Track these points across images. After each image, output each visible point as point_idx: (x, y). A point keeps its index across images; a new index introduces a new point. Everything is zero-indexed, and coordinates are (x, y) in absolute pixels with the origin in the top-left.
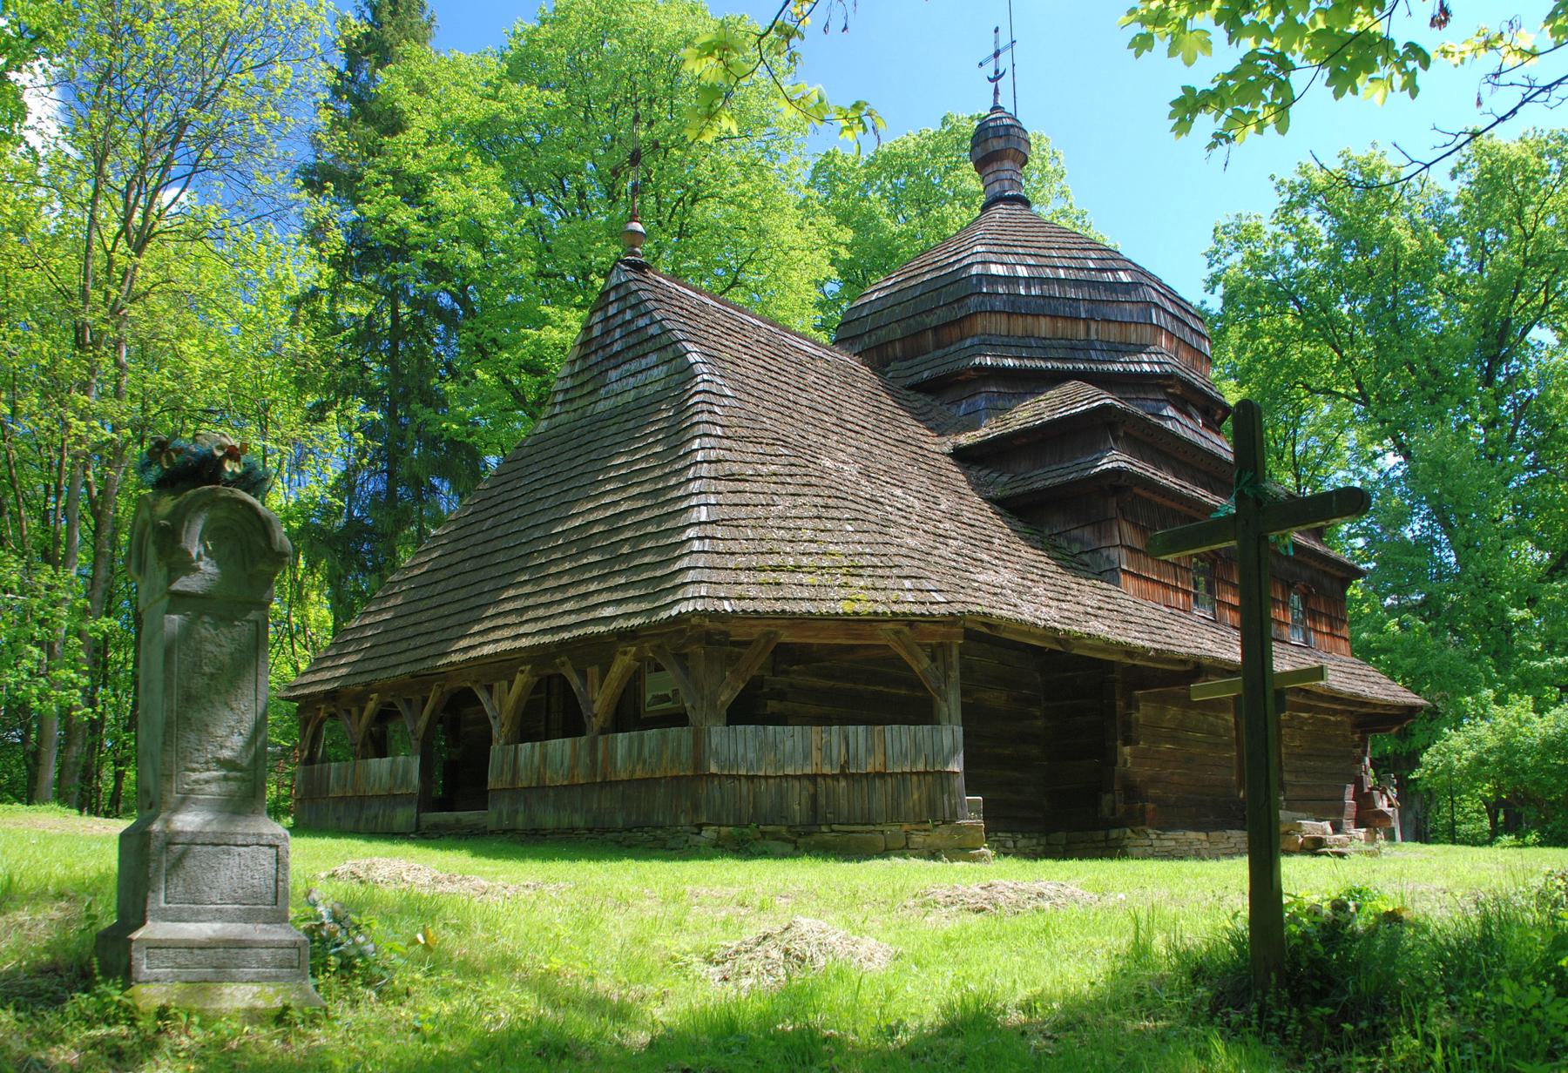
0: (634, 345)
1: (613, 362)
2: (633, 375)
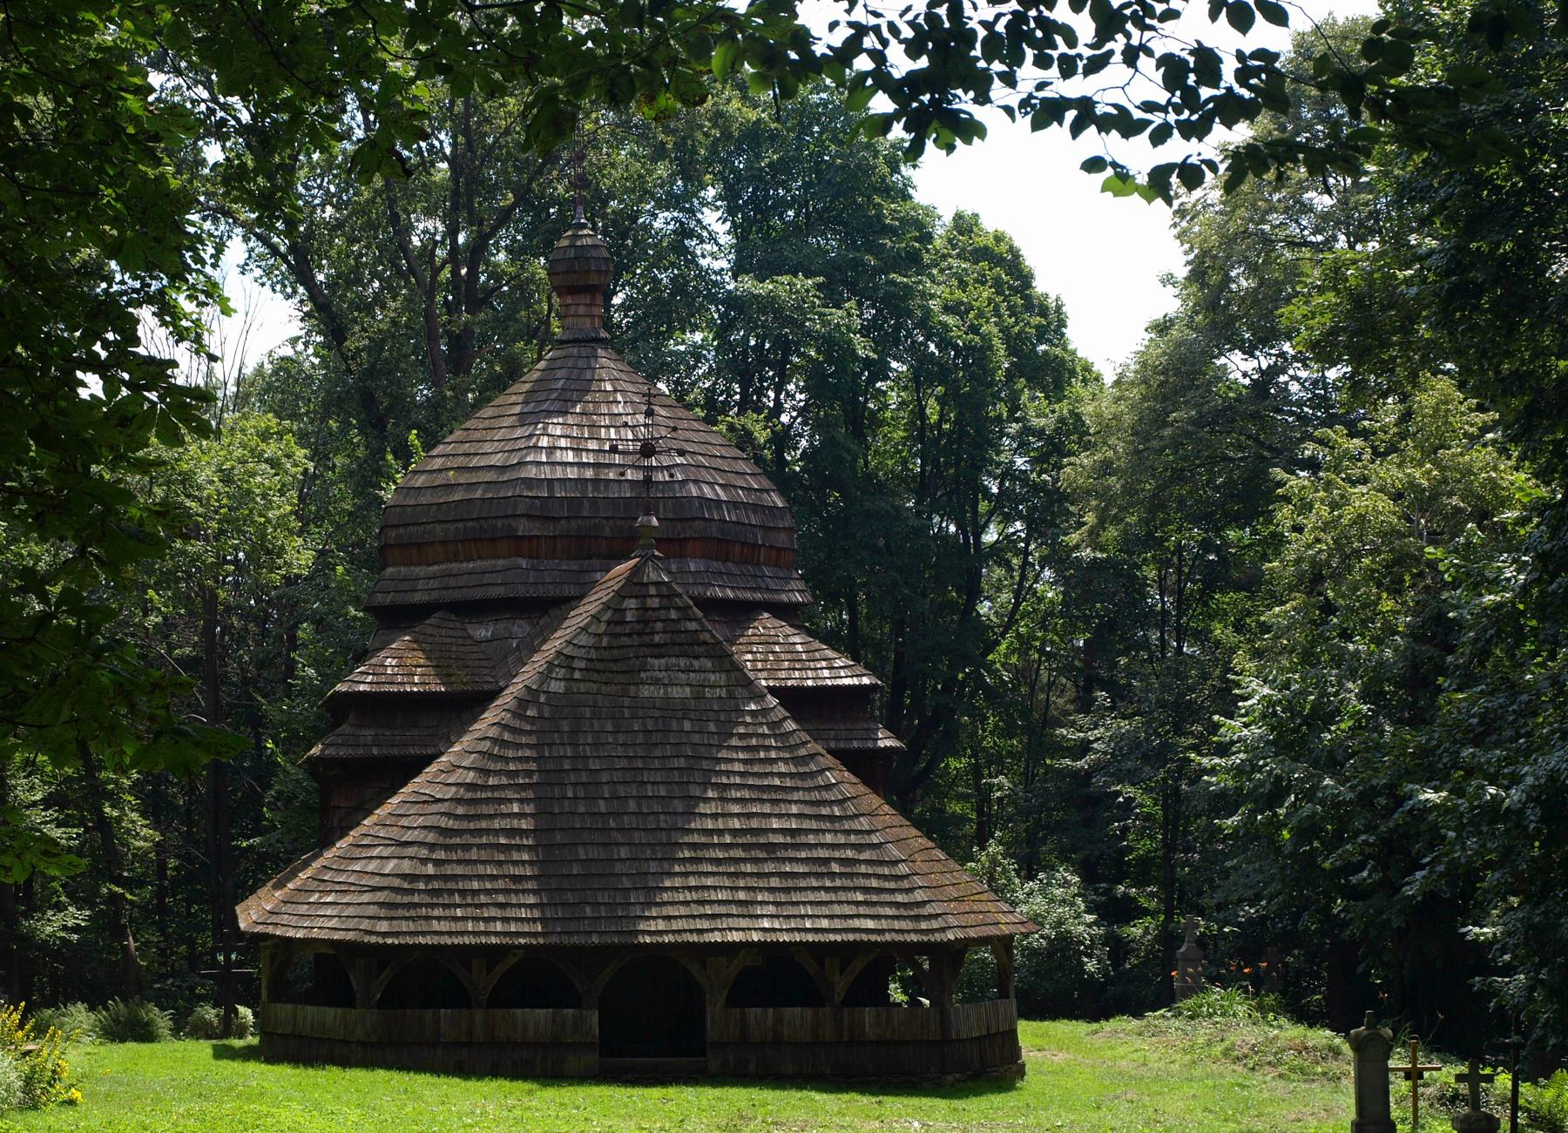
0: (680, 644)
1: (656, 651)
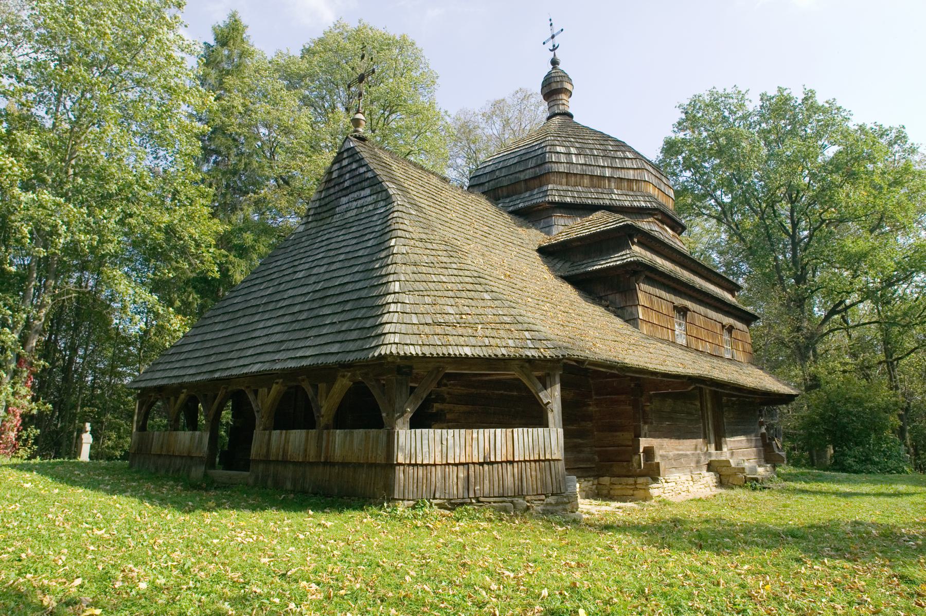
0: (357, 184)
1: (344, 192)
2: (355, 200)
